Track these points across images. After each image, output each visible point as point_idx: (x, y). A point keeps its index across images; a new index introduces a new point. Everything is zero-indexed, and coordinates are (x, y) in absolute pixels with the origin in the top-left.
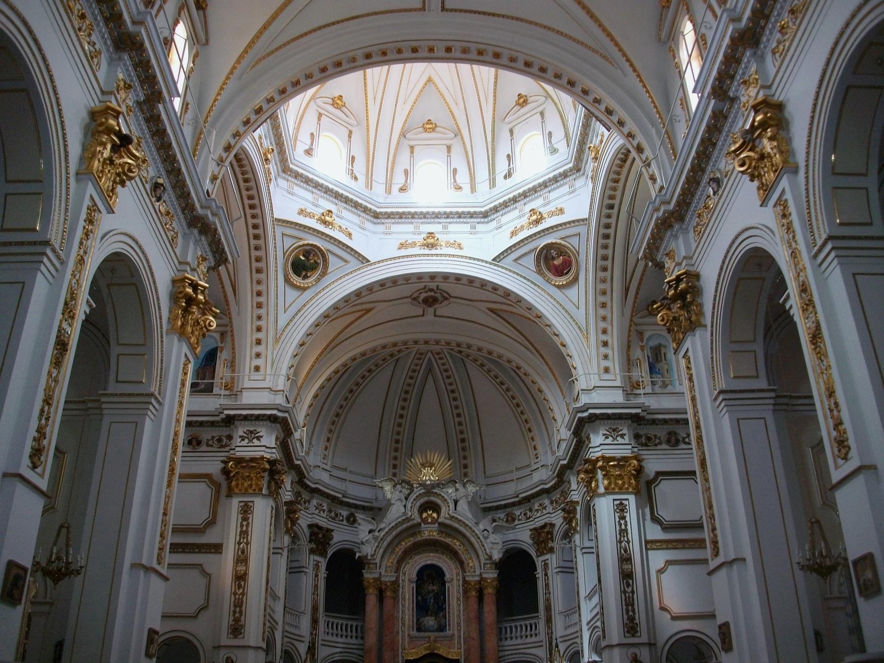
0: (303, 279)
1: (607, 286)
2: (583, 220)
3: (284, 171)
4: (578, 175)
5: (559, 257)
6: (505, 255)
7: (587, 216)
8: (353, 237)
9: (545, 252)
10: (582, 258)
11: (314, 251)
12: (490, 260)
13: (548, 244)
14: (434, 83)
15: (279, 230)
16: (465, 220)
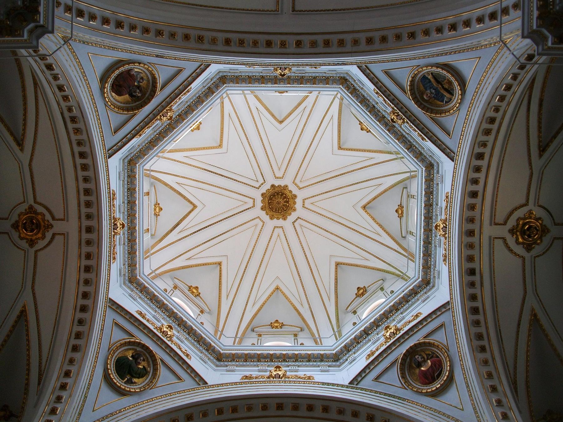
0: (125, 383)
1: (491, 368)
2: (444, 306)
3: (131, 281)
4: (428, 287)
5: (425, 361)
6: (363, 375)
7: (449, 299)
8: (191, 359)
9: (408, 360)
10: (453, 350)
11: (145, 355)
12: (347, 383)
13: (411, 347)
14: (281, 290)
15: (111, 316)
16: (315, 363)
